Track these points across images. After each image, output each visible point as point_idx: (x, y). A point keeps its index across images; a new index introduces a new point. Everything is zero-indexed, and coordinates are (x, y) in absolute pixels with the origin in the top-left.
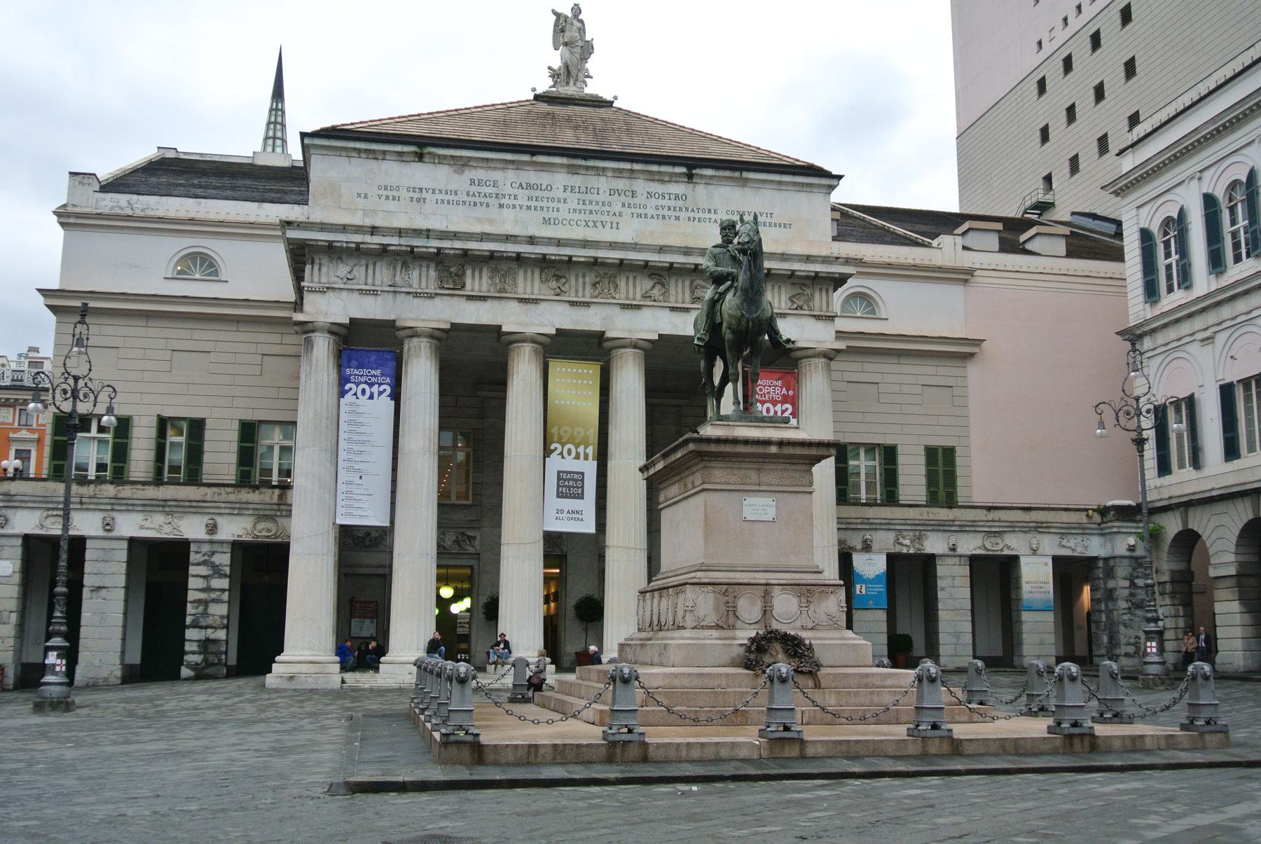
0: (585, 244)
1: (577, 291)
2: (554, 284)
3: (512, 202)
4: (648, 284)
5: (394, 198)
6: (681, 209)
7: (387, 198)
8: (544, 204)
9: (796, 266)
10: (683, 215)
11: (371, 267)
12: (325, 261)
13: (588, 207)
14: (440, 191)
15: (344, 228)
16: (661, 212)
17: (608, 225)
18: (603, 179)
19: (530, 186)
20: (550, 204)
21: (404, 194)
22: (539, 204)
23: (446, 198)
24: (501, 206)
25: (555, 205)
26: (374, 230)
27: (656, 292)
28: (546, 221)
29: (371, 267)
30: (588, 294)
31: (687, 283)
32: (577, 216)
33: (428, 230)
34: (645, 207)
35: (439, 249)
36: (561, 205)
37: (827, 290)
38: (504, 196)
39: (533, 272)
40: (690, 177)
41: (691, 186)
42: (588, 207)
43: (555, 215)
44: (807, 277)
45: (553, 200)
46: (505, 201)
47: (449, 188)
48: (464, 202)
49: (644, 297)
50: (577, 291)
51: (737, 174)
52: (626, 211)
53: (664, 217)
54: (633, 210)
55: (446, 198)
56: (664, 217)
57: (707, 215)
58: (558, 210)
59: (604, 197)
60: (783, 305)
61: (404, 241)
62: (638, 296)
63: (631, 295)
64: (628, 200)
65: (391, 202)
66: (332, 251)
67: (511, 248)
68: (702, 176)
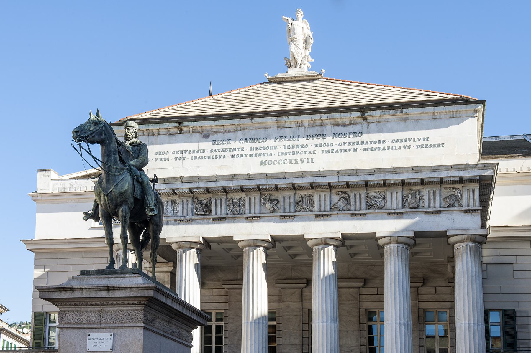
0: (284, 175)
1: (285, 209)
2: (268, 206)
3: (240, 153)
4: (335, 198)
5: (165, 159)
6: (358, 143)
7: (161, 160)
8: (262, 151)
9: (444, 174)
10: (360, 147)
13: (292, 150)
14: (194, 152)
16: (343, 147)
17: (305, 161)
18: (302, 129)
20: (266, 151)
21: (171, 156)
22: (258, 152)
23: (198, 155)
25: (269, 151)
27: (341, 204)
28: (263, 163)
30: (292, 209)
31: (363, 196)
32: (284, 157)
33: (181, 178)
34: (332, 145)
36: (273, 151)
38: (234, 150)
39: (255, 198)
40: (365, 119)
41: (365, 125)
42: (292, 150)
43: (269, 158)
44: (454, 182)
45: (268, 148)
46: (236, 153)
47: (200, 149)
48: (209, 157)
49: (332, 208)
50: (285, 209)
52: (318, 149)
53: (345, 151)
54: (323, 148)
55: (198, 155)
56: (345, 151)
57: (377, 145)
58: (271, 155)
60: (438, 205)
61: (167, 186)
62: (328, 208)
63: (322, 208)
65: (163, 162)
67: (236, 184)
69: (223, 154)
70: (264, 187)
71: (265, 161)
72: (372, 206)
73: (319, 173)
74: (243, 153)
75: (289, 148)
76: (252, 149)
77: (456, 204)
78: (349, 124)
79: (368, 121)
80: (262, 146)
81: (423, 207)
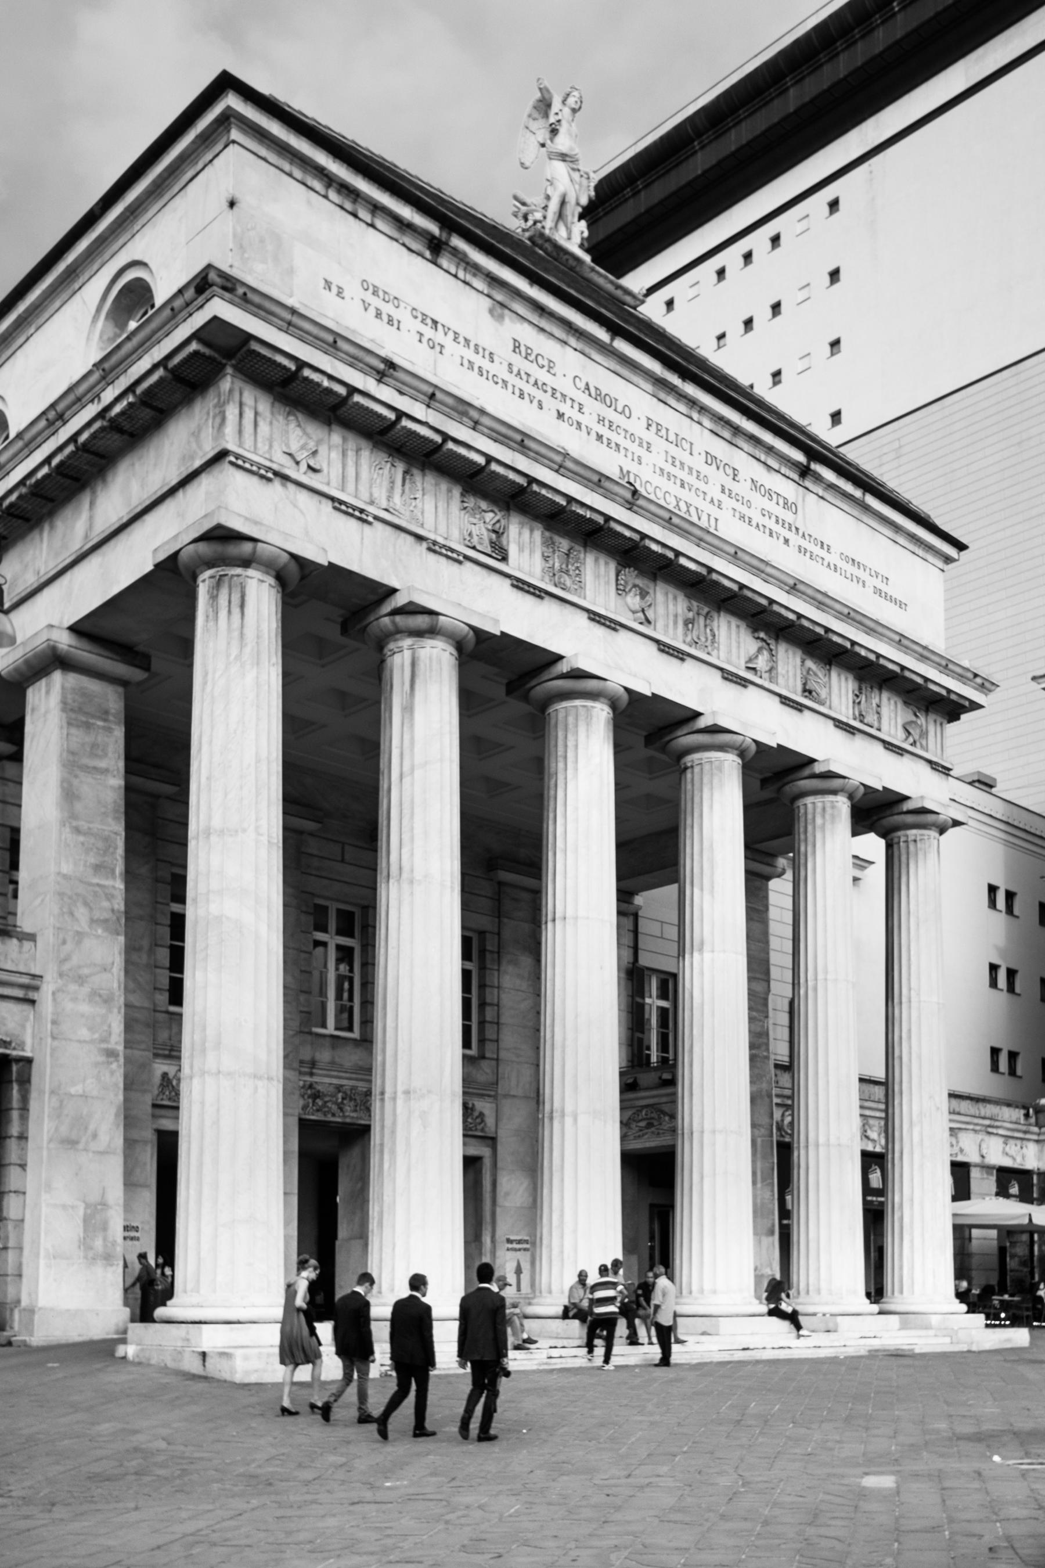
2: (633, 600)
3: (576, 416)
9: (932, 674)
11: (351, 454)
12: (264, 405)
15: (333, 342)
19: (599, 396)
24: (560, 416)
26: (387, 370)
27: (762, 662)
29: (351, 454)
33: (482, 412)
35: (490, 459)
37: (941, 724)
40: (804, 472)
51: (858, 493)
52: (724, 498)
59: (698, 462)
64: (729, 483)
66: (292, 390)
68: (818, 478)
69: (538, 394)
70: (654, 547)
71: (628, 472)
72: (810, 692)
73: (762, 566)
74: (584, 420)
75: (673, 464)
76: (601, 420)
77: (918, 744)
78: (778, 472)
79: (808, 483)
80: (623, 426)
81: (879, 730)
